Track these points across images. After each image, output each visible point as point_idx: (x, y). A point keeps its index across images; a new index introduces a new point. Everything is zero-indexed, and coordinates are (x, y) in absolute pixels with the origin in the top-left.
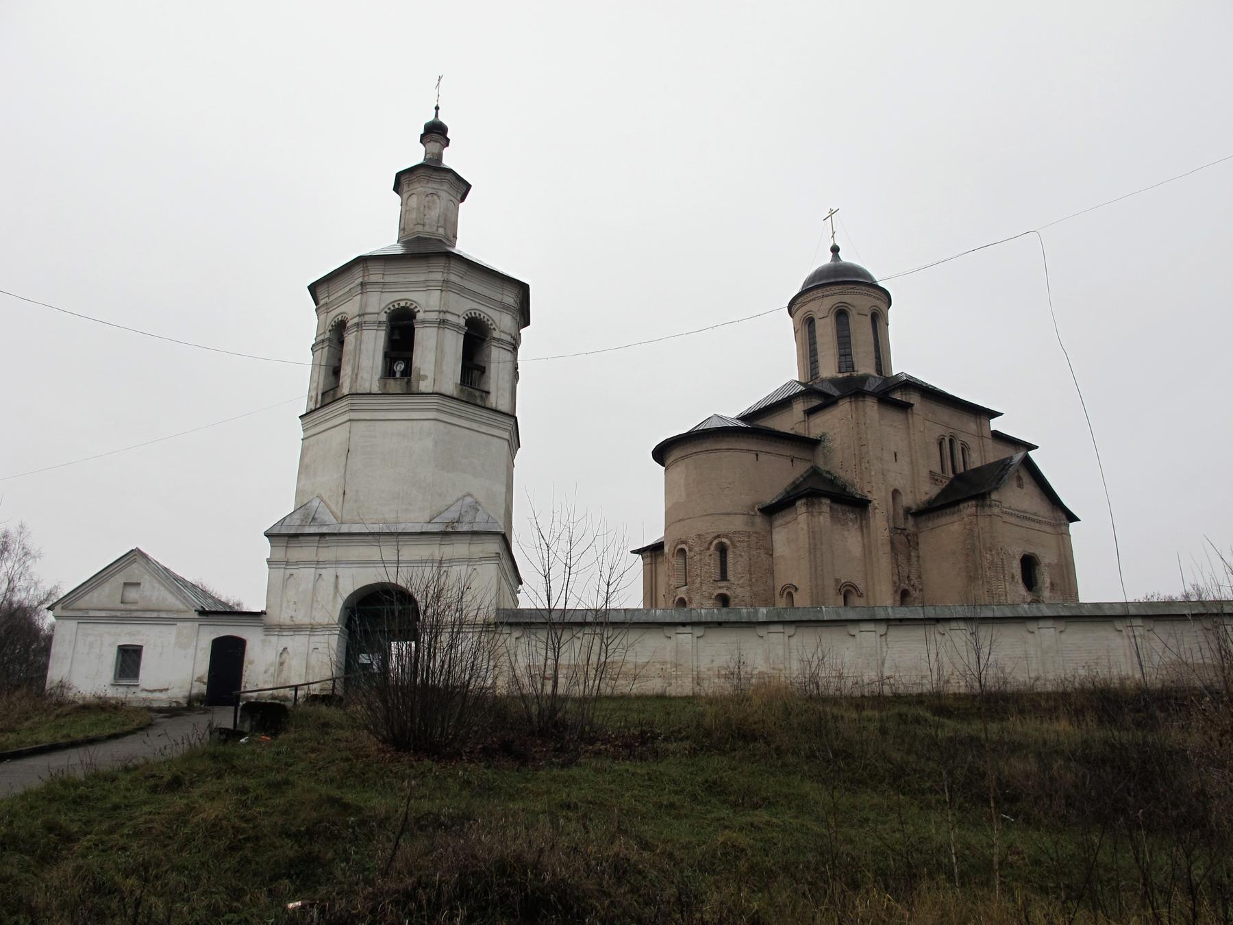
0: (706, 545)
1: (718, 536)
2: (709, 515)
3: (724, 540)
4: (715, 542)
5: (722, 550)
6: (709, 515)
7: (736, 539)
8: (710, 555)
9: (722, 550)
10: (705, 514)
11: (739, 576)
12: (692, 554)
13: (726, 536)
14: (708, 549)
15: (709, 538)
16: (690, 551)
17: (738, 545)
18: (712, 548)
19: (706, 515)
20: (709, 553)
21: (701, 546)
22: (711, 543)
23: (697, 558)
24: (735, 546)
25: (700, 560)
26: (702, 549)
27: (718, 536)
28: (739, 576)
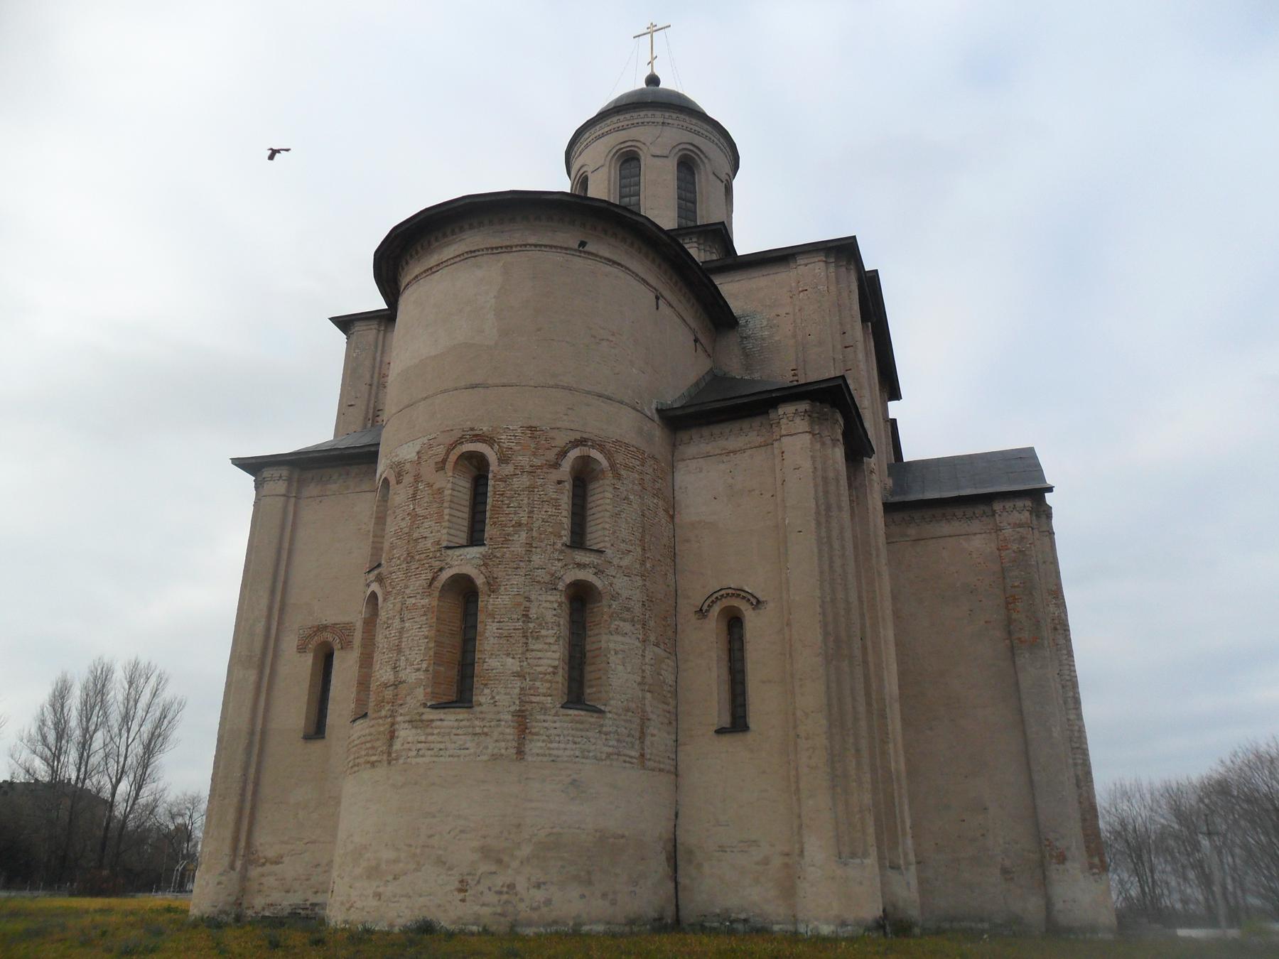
0: (551, 455)
1: (581, 442)
2: (563, 388)
3: (595, 454)
4: (574, 453)
5: (583, 479)
6: (563, 388)
7: (620, 459)
8: (559, 482)
9: (583, 479)
10: (551, 383)
11: (623, 546)
12: (509, 469)
13: (601, 448)
14: (556, 465)
15: (561, 440)
16: (503, 460)
17: (623, 472)
18: (567, 465)
19: (557, 386)
20: (555, 475)
21: (534, 454)
22: (563, 454)
23: (522, 481)
24: (618, 476)
25: (531, 489)
26: (537, 462)
27: (581, 442)
28: (623, 546)
